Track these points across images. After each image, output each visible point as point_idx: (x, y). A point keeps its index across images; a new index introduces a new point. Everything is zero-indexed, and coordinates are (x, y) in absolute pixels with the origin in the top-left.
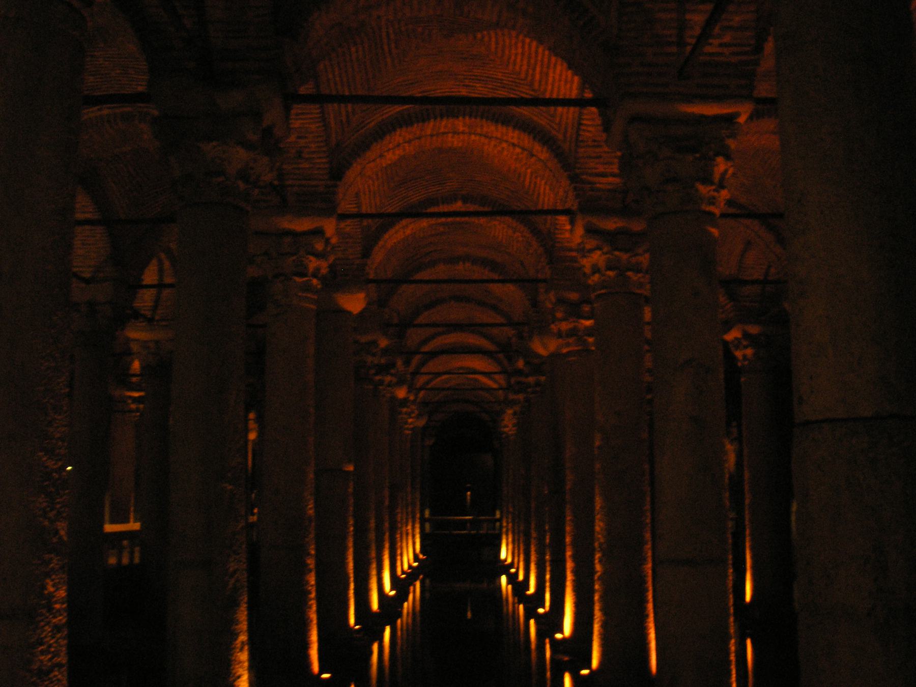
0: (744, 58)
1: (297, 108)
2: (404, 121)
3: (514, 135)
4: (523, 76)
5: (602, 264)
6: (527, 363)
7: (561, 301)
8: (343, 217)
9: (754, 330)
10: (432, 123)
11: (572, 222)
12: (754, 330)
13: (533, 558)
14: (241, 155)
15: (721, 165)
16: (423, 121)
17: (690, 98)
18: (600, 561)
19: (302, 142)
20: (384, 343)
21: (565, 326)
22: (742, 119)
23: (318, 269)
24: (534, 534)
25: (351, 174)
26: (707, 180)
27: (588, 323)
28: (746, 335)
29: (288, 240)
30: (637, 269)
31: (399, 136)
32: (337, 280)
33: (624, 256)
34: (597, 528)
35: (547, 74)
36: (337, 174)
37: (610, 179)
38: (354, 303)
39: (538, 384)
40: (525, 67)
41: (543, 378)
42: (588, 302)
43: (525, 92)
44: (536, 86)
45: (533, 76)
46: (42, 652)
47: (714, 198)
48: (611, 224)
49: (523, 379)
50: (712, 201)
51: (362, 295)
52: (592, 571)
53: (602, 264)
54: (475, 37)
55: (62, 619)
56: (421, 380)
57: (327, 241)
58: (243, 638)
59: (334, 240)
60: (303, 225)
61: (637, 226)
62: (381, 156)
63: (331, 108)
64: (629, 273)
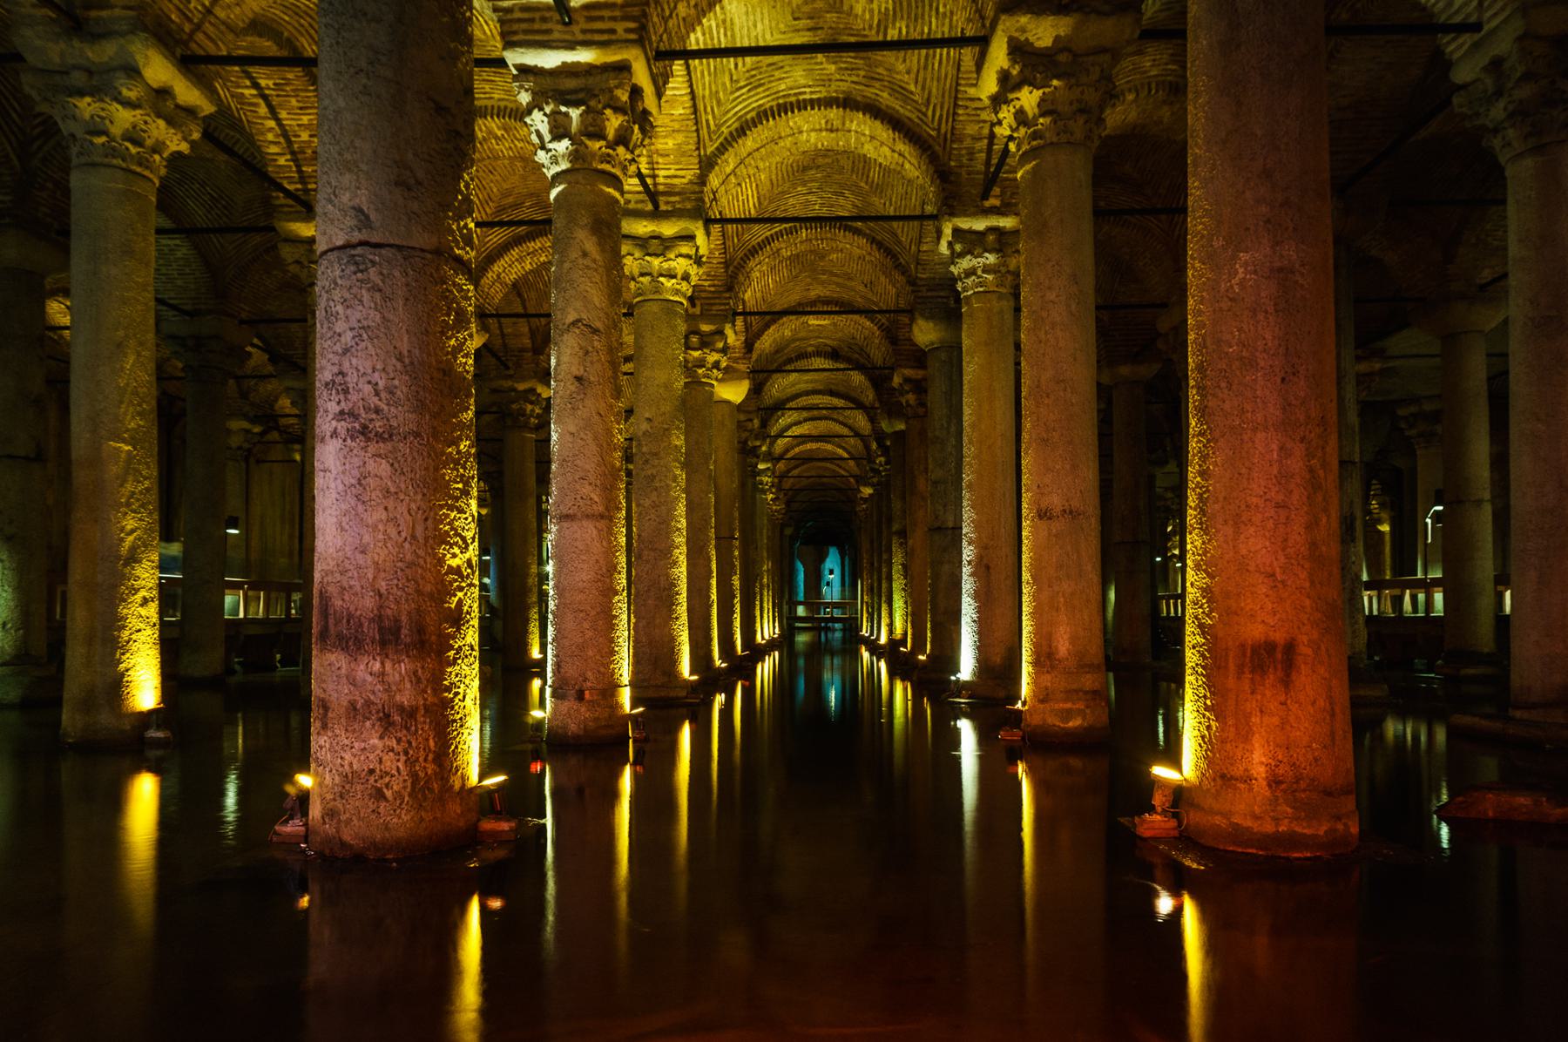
5: (636, 272)
14: (123, 118)
26: (600, 136)
27: (696, 354)
28: (907, 380)
33: (656, 262)
48: (642, 228)
50: (607, 159)
53: (636, 272)
61: (669, 229)
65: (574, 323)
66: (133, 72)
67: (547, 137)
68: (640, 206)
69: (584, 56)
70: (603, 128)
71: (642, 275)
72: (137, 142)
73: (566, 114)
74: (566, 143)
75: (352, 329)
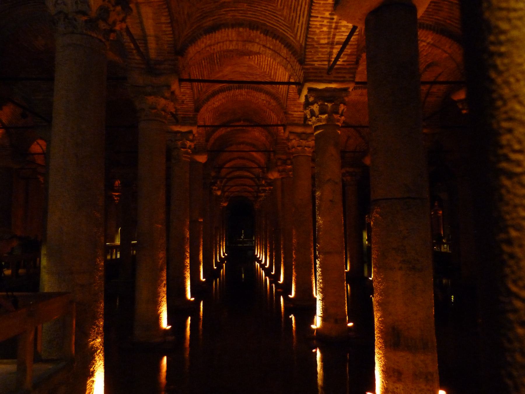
0: (352, 66)
1: (183, 84)
2: (221, 91)
3: (263, 96)
4: (267, 73)
5: (296, 145)
6: (266, 182)
7: (279, 159)
8: (199, 126)
9: (351, 170)
10: (233, 91)
11: (284, 130)
12: (351, 170)
13: (268, 254)
14: (163, 102)
15: (342, 107)
16: (230, 90)
17: (330, 82)
18: (295, 254)
19: (184, 97)
20: (213, 174)
21: (281, 168)
22: (350, 90)
23: (190, 146)
24: (268, 245)
25: (203, 110)
26: (337, 113)
29: (179, 134)
30: (309, 147)
31: (220, 96)
32: (196, 151)
33: (304, 143)
34: (294, 242)
35: (276, 73)
36: (197, 110)
37: (299, 113)
38: (202, 159)
39: (270, 190)
40: (268, 70)
41: (272, 188)
42: (289, 159)
43: (268, 79)
44: (272, 77)
45: (271, 73)
46: (95, 286)
47: (339, 119)
48: (299, 130)
49: (264, 188)
50: (338, 121)
51: (206, 156)
52: (292, 257)
53: (296, 145)
54: (249, 58)
55: (102, 273)
56: (226, 189)
57: (194, 135)
58: (165, 282)
59: (196, 135)
60: (184, 129)
62: (214, 103)
63: (195, 84)
64: (306, 148)
65: (329, 180)
66: (169, 87)
67: (317, 112)
68: (299, 122)
69: (333, 86)
70: (339, 110)
71: (298, 146)
72: (164, 111)
73: (327, 105)
74: (326, 115)
75: (407, 230)
